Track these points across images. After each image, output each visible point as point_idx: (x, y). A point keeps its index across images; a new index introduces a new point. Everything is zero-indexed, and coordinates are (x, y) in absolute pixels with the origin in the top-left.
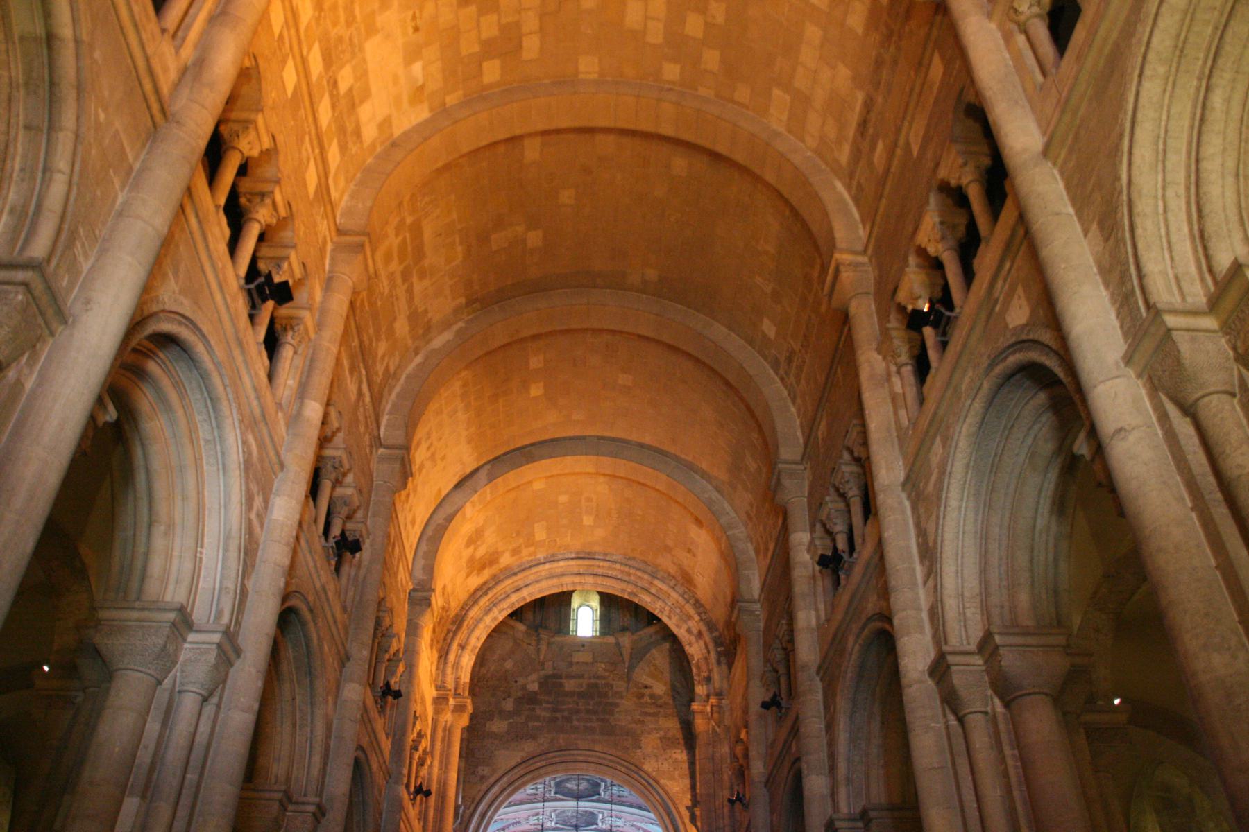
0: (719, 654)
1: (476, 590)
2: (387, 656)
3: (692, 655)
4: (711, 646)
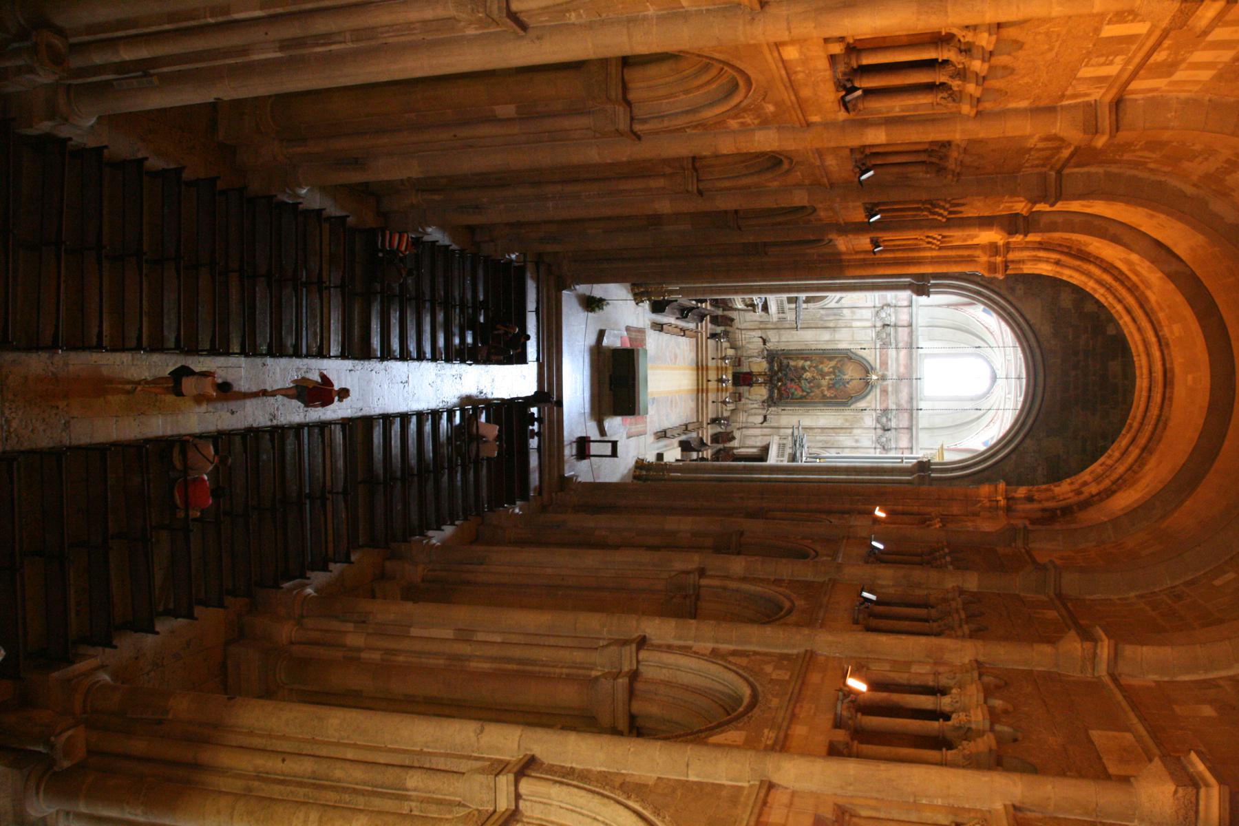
3: (1059, 486)
4: (1062, 504)
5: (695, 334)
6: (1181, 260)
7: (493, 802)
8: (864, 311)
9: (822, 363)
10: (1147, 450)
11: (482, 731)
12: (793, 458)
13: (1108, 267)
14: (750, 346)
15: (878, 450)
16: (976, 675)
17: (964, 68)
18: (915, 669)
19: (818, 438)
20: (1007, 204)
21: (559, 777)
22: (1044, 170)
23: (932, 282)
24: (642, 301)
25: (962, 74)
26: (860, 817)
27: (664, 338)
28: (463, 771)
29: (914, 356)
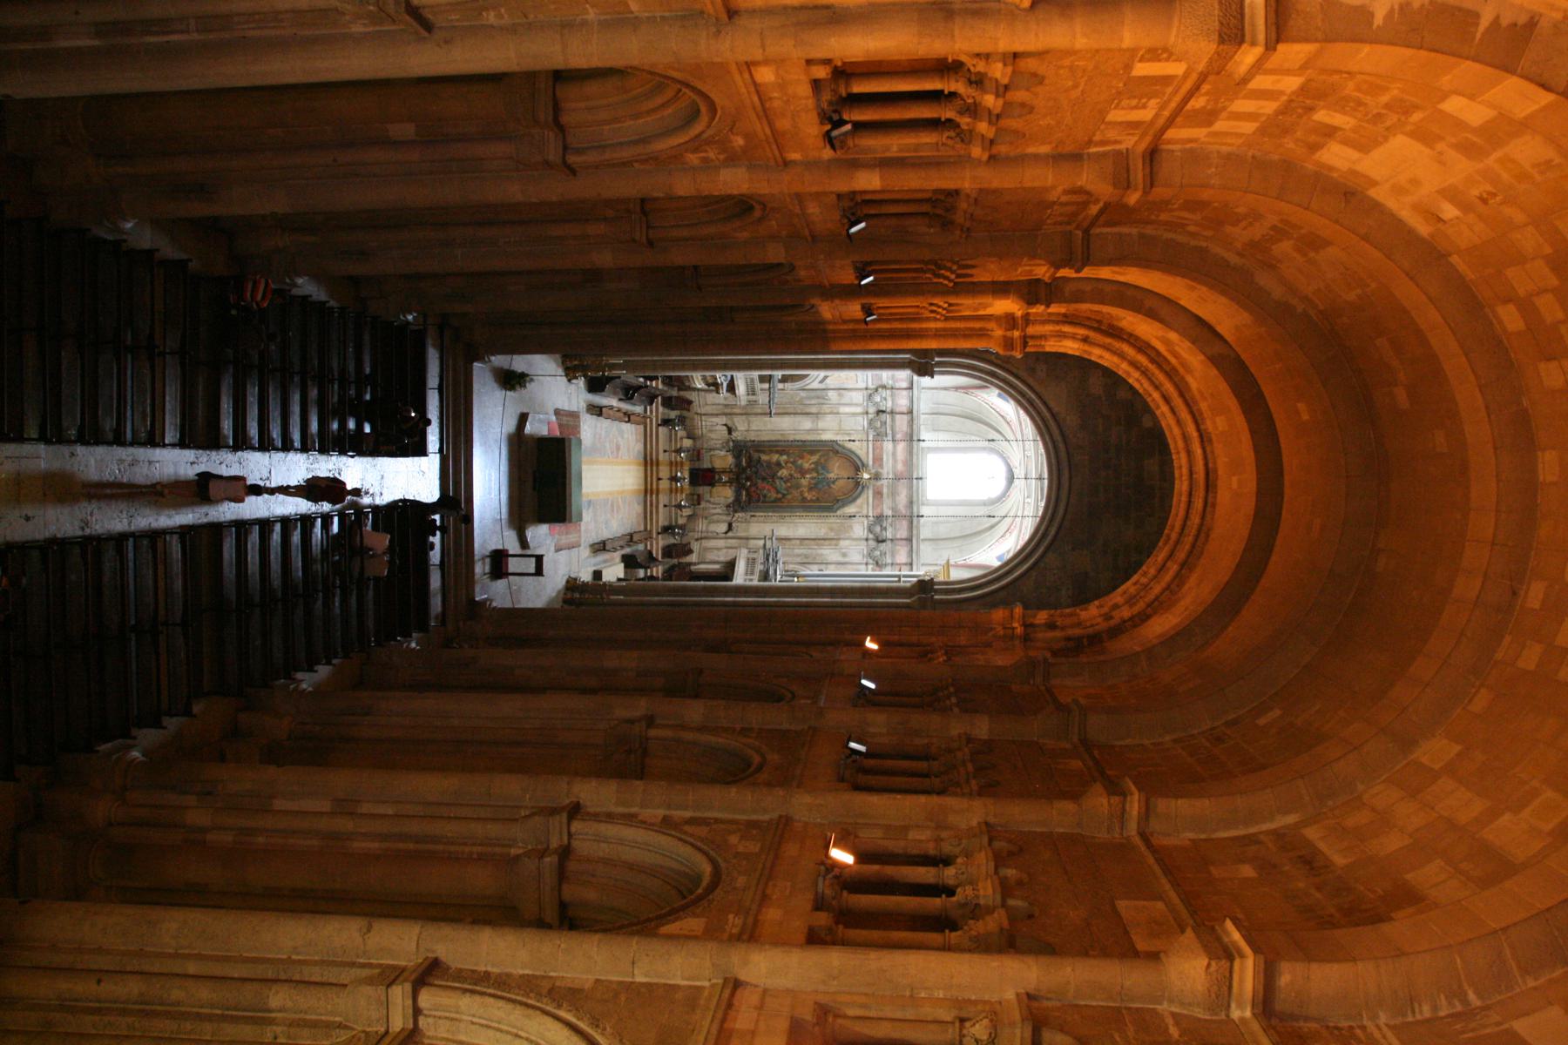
3: (1086, 609)
4: (1090, 630)
5: (643, 420)
6: (1226, 342)
7: (385, 1020)
8: (854, 394)
9: (802, 458)
10: (1187, 566)
11: (369, 931)
12: (765, 576)
13: (1143, 347)
14: (713, 436)
15: (870, 567)
16: (985, 840)
17: (975, 103)
18: (912, 835)
19: (797, 551)
20: (1028, 268)
21: (470, 984)
22: (1069, 228)
23: (937, 359)
24: (576, 378)
25: (973, 110)
26: (845, 1017)
27: (603, 424)
28: (345, 982)
29: (915, 450)
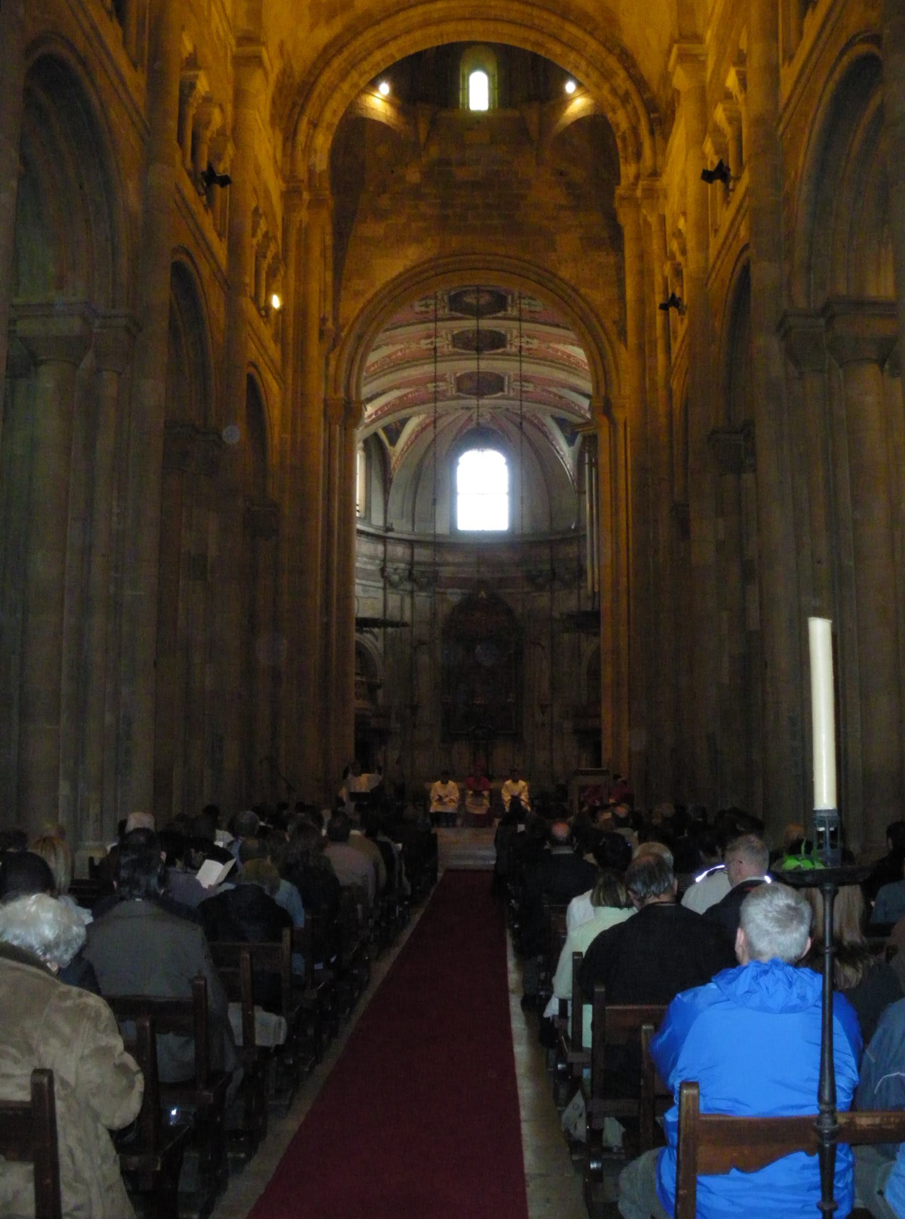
0: (651, 122)
1: (326, 49)
2: (208, 134)
3: (618, 125)
4: (641, 111)
8: (390, 604)
29: (452, 540)
